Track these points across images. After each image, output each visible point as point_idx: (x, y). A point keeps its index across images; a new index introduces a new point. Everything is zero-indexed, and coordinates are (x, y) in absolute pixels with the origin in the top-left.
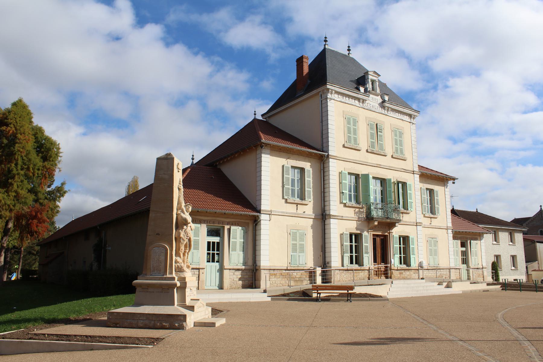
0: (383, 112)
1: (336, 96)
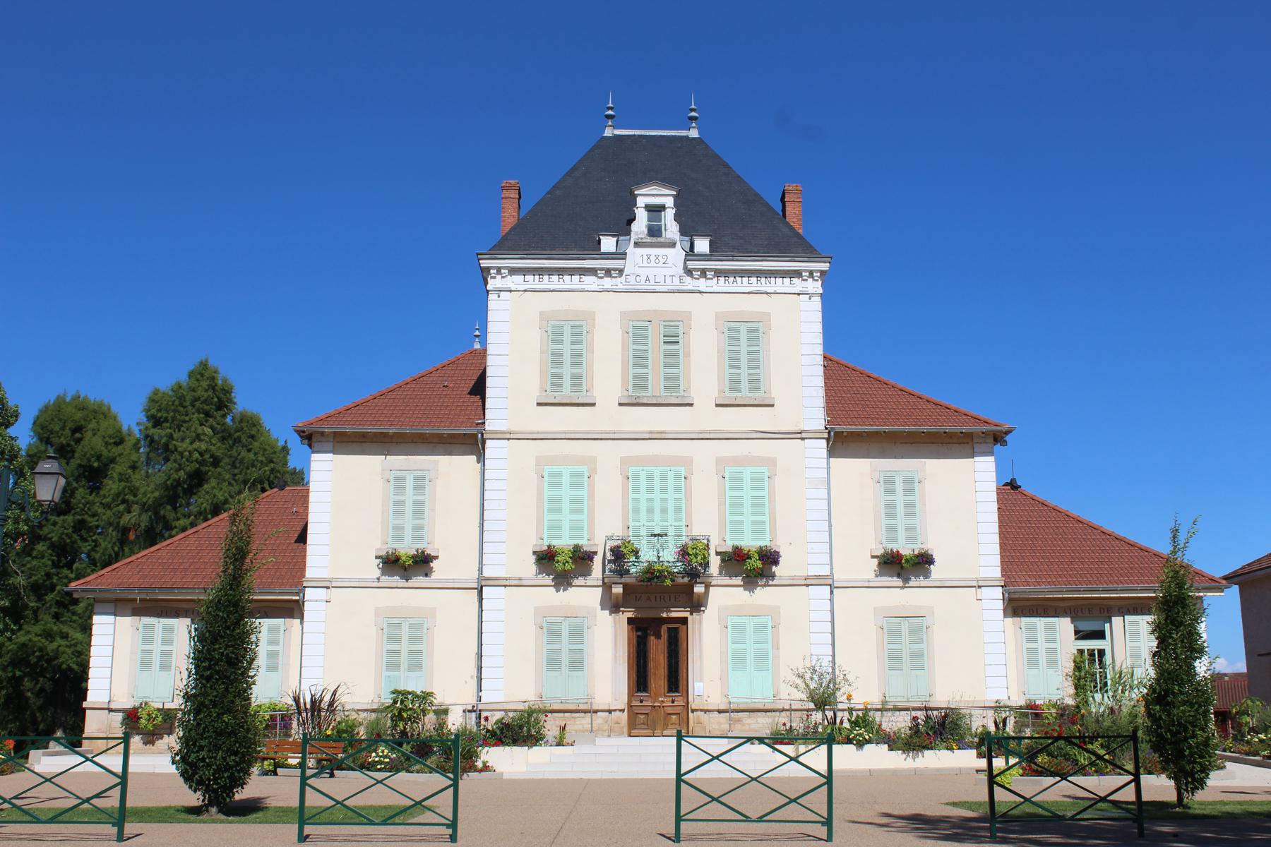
0: (690, 287)
1: (518, 279)
